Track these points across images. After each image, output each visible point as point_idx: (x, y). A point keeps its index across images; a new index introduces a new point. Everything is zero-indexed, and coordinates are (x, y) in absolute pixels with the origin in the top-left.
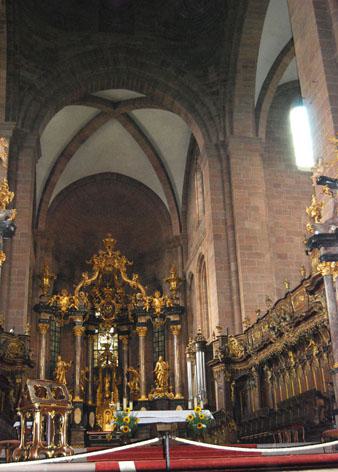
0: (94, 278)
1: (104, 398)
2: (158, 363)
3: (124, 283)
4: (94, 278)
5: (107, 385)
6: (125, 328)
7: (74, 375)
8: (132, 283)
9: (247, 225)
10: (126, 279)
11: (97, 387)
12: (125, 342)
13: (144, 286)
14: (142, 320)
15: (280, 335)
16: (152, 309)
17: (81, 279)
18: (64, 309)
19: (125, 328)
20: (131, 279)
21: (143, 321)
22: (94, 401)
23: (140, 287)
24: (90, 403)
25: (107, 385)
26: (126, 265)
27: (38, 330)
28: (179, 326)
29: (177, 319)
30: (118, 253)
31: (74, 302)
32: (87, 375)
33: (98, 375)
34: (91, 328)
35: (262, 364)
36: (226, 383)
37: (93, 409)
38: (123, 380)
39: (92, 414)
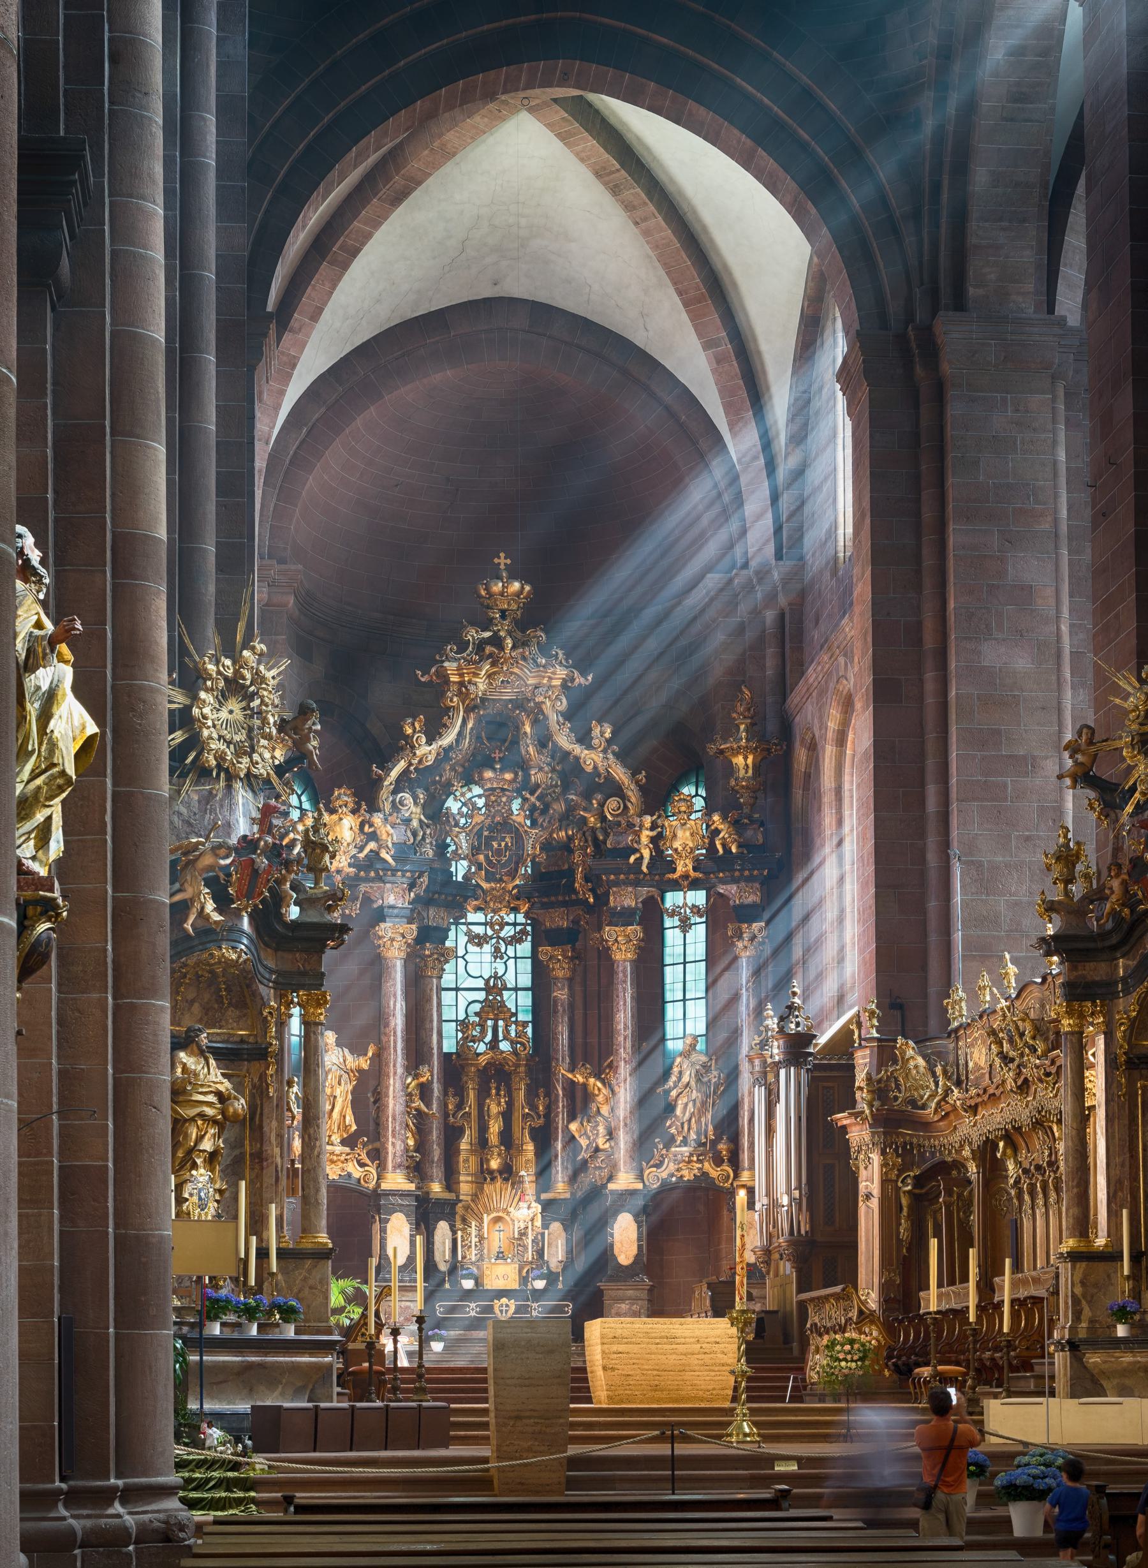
1: (484, 1175)
4: (448, 739)
5: (495, 1128)
6: (559, 920)
7: (379, 1098)
8: (591, 758)
9: (993, 654)
10: (564, 740)
11: (460, 1131)
12: (561, 971)
15: (1024, 1087)
17: (398, 745)
19: (559, 920)
20: (584, 739)
21: (629, 902)
22: (450, 1183)
23: (620, 773)
24: (436, 1188)
25: (495, 1128)
29: (752, 898)
31: (373, 836)
32: (424, 1091)
33: (461, 1093)
34: (434, 916)
35: (989, 1145)
36: (885, 1182)
37: (447, 1210)
38: (549, 1109)
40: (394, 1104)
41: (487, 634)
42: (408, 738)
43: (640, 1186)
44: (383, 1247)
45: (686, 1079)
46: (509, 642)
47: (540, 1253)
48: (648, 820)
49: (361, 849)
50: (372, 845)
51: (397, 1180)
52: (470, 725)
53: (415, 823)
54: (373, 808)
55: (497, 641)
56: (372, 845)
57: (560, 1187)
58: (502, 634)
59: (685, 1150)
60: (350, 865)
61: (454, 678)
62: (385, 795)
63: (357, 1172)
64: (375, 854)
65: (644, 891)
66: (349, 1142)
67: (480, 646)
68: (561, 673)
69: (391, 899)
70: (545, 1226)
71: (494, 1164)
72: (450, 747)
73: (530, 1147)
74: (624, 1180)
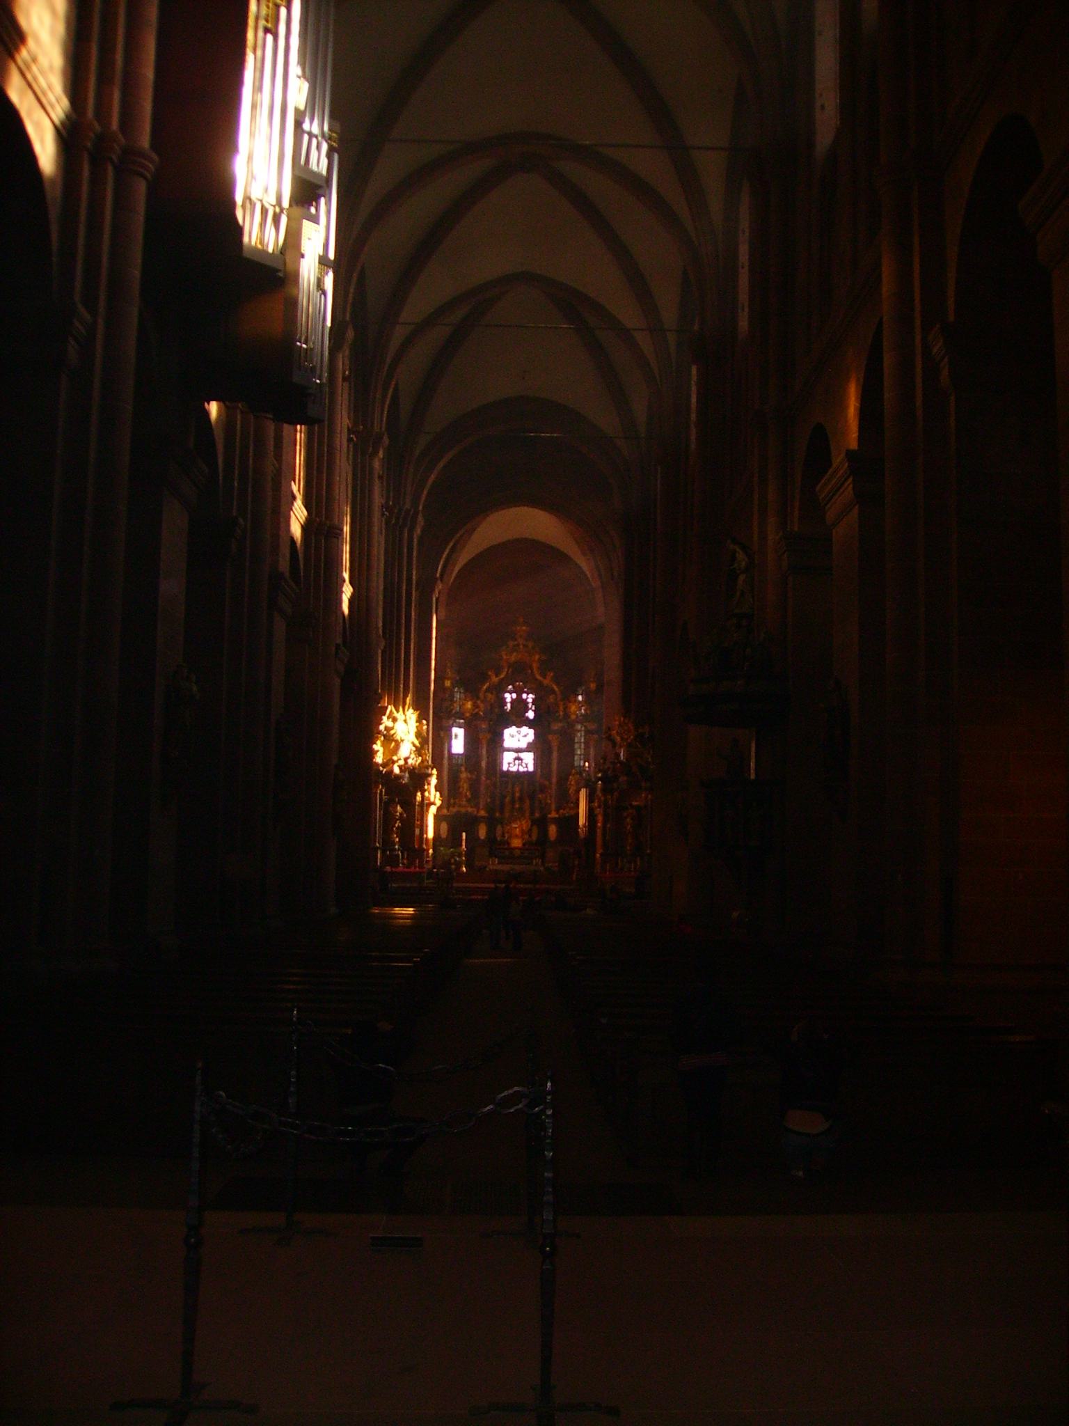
0: (502, 676)
2: (571, 777)
3: (536, 680)
5: (517, 795)
8: (546, 682)
10: (538, 677)
11: (506, 797)
13: (558, 684)
14: (556, 726)
16: (567, 715)
18: (468, 715)
20: (544, 677)
22: (502, 812)
23: (555, 687)
24: (497, 815)
25: (517, 795)
26: (539, 659)
27: (439, 735)
28: (596, 736)
30: (530, 644)
39: (499, 827)
40: (482, 789)
41: (516, 643)
42: (490, 676)
43: (557, 816)
44: (478, 833)
45: (572, 783)
46: (521, 647)
47: (530, 836)
48: (562, 703)
49: (473, 710)
50: (477, 710)
51: (482, 813)
52: (510, 670)
53: (492, 701)
54: (478, 698)
55: (518, 645)
56: (477, 710)
57: (537, 815)
58: (521, 643)
59: (572, 805)
60: (471, 716)
61: (505, 657)
62: (481, 695)
63: (470, 810)
64: (477, 713)
65: (560, 725)
66: (468, 800)
67: (514, 646)
68: (537, 657)
69: (484, 726)
70: (532, 826)
71: (517, 806)
72: (503, 679)
73: (528, 802)
74: (554, 815)
